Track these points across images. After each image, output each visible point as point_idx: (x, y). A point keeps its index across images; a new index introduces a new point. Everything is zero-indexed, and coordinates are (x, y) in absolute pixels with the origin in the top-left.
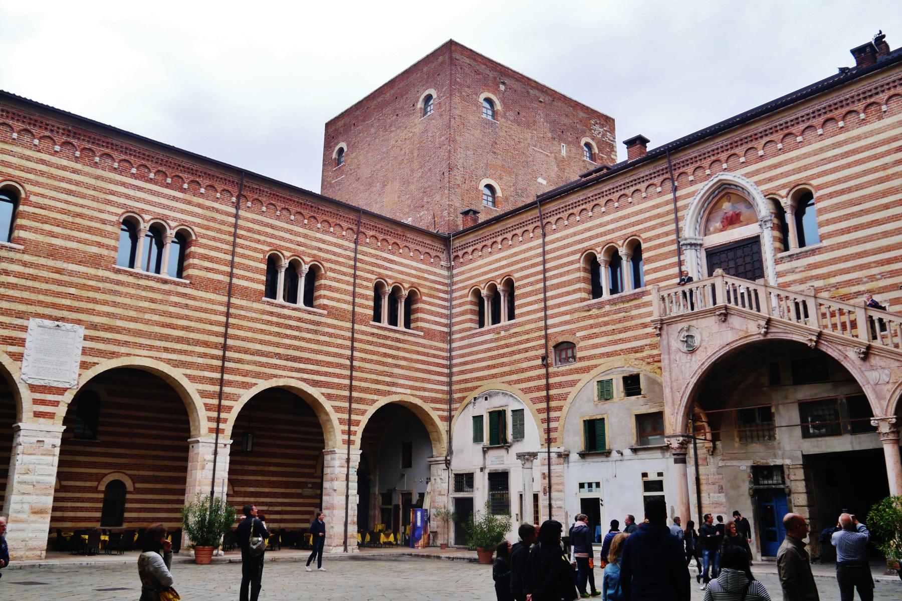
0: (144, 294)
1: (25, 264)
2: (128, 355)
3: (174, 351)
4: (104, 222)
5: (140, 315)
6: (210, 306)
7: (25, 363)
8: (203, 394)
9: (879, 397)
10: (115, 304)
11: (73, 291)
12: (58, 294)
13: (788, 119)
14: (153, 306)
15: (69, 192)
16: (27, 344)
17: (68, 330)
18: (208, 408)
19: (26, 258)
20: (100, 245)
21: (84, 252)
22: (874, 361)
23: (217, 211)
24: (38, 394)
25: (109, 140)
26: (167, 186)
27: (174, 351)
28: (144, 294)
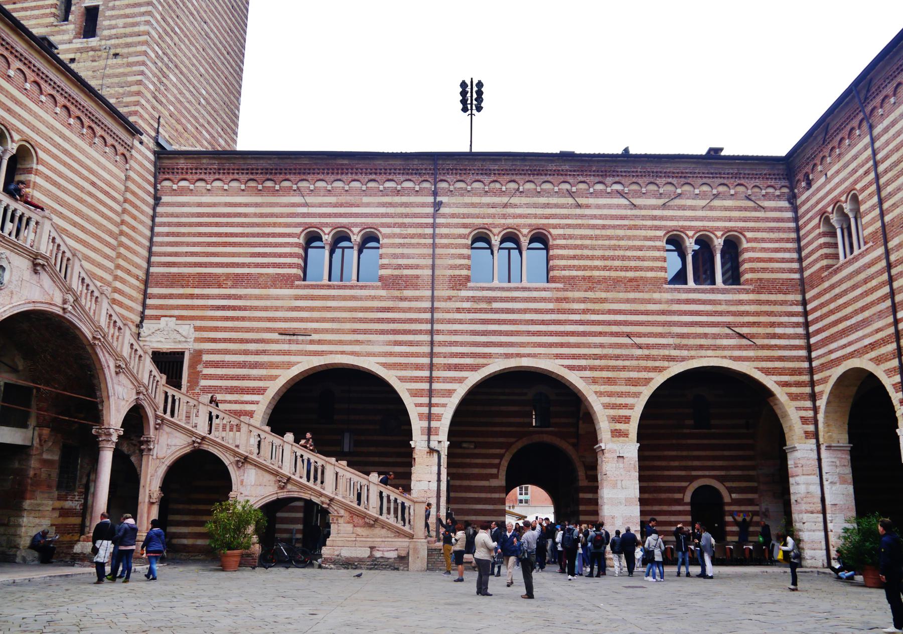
9: (118, 411)
13: (42, 69)
22: (122, 377)
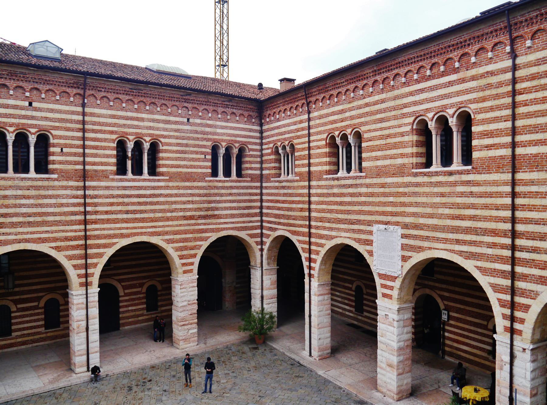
0: (436, 190)
1: (368, 186)
2: (430, 248)
3: (464, 242)
4: (402, 135)
5: (435, 211)
6: (494, 189)
7: (375, 258)
8: (496, 288)
10: (417, 204)
11: (391, 199)
12: (385, 204)
14: (444, 200)
15: (381, 120)
16: (374, 244)
17: (392, 232)
18: (502, 303)
19: (368, 181)
20: (402, 156)
21: (394, 166)
23: (492, 73)
24: (383, 281)
25: (397, 61)
26: (443, 74)
27: (464, 242)
28: (436, 190)
